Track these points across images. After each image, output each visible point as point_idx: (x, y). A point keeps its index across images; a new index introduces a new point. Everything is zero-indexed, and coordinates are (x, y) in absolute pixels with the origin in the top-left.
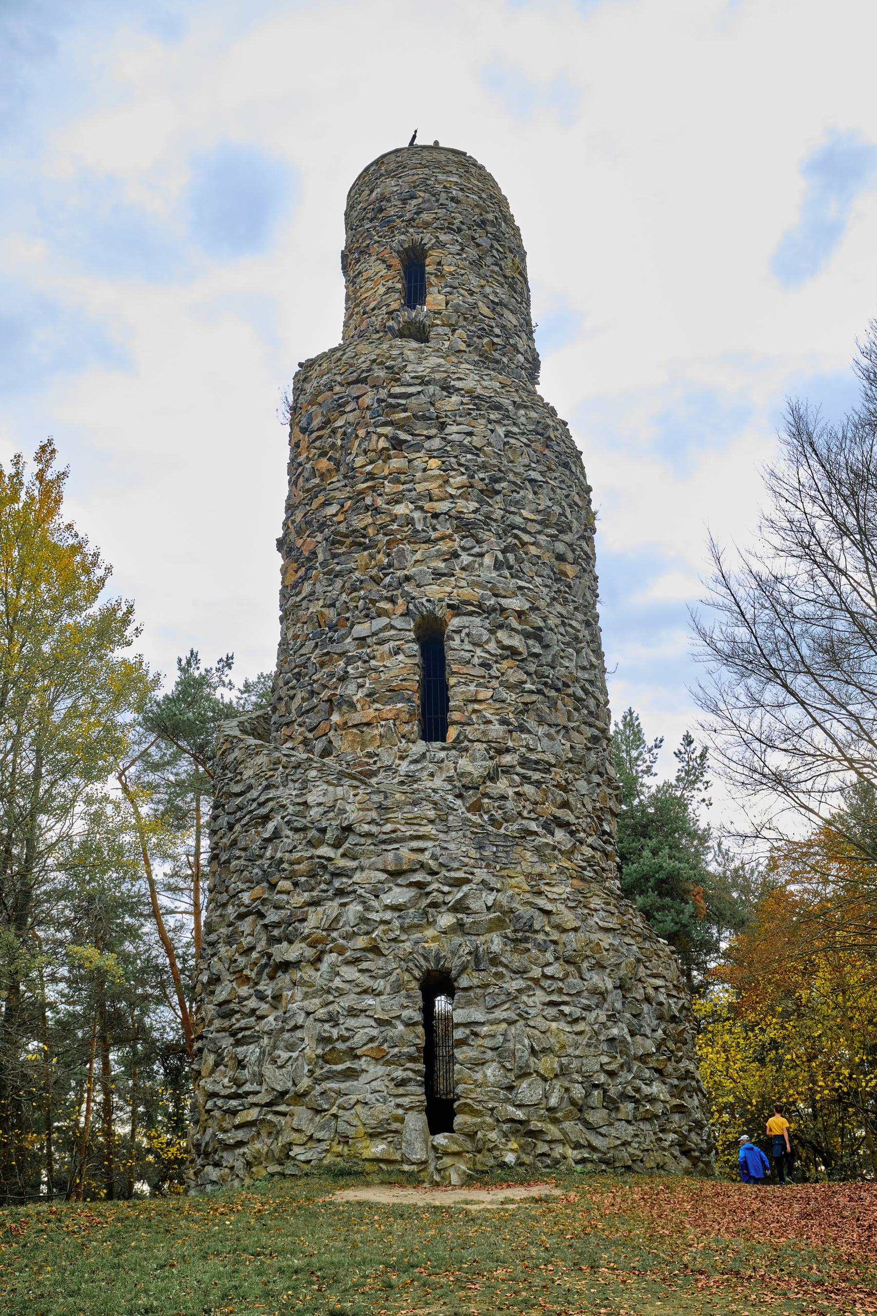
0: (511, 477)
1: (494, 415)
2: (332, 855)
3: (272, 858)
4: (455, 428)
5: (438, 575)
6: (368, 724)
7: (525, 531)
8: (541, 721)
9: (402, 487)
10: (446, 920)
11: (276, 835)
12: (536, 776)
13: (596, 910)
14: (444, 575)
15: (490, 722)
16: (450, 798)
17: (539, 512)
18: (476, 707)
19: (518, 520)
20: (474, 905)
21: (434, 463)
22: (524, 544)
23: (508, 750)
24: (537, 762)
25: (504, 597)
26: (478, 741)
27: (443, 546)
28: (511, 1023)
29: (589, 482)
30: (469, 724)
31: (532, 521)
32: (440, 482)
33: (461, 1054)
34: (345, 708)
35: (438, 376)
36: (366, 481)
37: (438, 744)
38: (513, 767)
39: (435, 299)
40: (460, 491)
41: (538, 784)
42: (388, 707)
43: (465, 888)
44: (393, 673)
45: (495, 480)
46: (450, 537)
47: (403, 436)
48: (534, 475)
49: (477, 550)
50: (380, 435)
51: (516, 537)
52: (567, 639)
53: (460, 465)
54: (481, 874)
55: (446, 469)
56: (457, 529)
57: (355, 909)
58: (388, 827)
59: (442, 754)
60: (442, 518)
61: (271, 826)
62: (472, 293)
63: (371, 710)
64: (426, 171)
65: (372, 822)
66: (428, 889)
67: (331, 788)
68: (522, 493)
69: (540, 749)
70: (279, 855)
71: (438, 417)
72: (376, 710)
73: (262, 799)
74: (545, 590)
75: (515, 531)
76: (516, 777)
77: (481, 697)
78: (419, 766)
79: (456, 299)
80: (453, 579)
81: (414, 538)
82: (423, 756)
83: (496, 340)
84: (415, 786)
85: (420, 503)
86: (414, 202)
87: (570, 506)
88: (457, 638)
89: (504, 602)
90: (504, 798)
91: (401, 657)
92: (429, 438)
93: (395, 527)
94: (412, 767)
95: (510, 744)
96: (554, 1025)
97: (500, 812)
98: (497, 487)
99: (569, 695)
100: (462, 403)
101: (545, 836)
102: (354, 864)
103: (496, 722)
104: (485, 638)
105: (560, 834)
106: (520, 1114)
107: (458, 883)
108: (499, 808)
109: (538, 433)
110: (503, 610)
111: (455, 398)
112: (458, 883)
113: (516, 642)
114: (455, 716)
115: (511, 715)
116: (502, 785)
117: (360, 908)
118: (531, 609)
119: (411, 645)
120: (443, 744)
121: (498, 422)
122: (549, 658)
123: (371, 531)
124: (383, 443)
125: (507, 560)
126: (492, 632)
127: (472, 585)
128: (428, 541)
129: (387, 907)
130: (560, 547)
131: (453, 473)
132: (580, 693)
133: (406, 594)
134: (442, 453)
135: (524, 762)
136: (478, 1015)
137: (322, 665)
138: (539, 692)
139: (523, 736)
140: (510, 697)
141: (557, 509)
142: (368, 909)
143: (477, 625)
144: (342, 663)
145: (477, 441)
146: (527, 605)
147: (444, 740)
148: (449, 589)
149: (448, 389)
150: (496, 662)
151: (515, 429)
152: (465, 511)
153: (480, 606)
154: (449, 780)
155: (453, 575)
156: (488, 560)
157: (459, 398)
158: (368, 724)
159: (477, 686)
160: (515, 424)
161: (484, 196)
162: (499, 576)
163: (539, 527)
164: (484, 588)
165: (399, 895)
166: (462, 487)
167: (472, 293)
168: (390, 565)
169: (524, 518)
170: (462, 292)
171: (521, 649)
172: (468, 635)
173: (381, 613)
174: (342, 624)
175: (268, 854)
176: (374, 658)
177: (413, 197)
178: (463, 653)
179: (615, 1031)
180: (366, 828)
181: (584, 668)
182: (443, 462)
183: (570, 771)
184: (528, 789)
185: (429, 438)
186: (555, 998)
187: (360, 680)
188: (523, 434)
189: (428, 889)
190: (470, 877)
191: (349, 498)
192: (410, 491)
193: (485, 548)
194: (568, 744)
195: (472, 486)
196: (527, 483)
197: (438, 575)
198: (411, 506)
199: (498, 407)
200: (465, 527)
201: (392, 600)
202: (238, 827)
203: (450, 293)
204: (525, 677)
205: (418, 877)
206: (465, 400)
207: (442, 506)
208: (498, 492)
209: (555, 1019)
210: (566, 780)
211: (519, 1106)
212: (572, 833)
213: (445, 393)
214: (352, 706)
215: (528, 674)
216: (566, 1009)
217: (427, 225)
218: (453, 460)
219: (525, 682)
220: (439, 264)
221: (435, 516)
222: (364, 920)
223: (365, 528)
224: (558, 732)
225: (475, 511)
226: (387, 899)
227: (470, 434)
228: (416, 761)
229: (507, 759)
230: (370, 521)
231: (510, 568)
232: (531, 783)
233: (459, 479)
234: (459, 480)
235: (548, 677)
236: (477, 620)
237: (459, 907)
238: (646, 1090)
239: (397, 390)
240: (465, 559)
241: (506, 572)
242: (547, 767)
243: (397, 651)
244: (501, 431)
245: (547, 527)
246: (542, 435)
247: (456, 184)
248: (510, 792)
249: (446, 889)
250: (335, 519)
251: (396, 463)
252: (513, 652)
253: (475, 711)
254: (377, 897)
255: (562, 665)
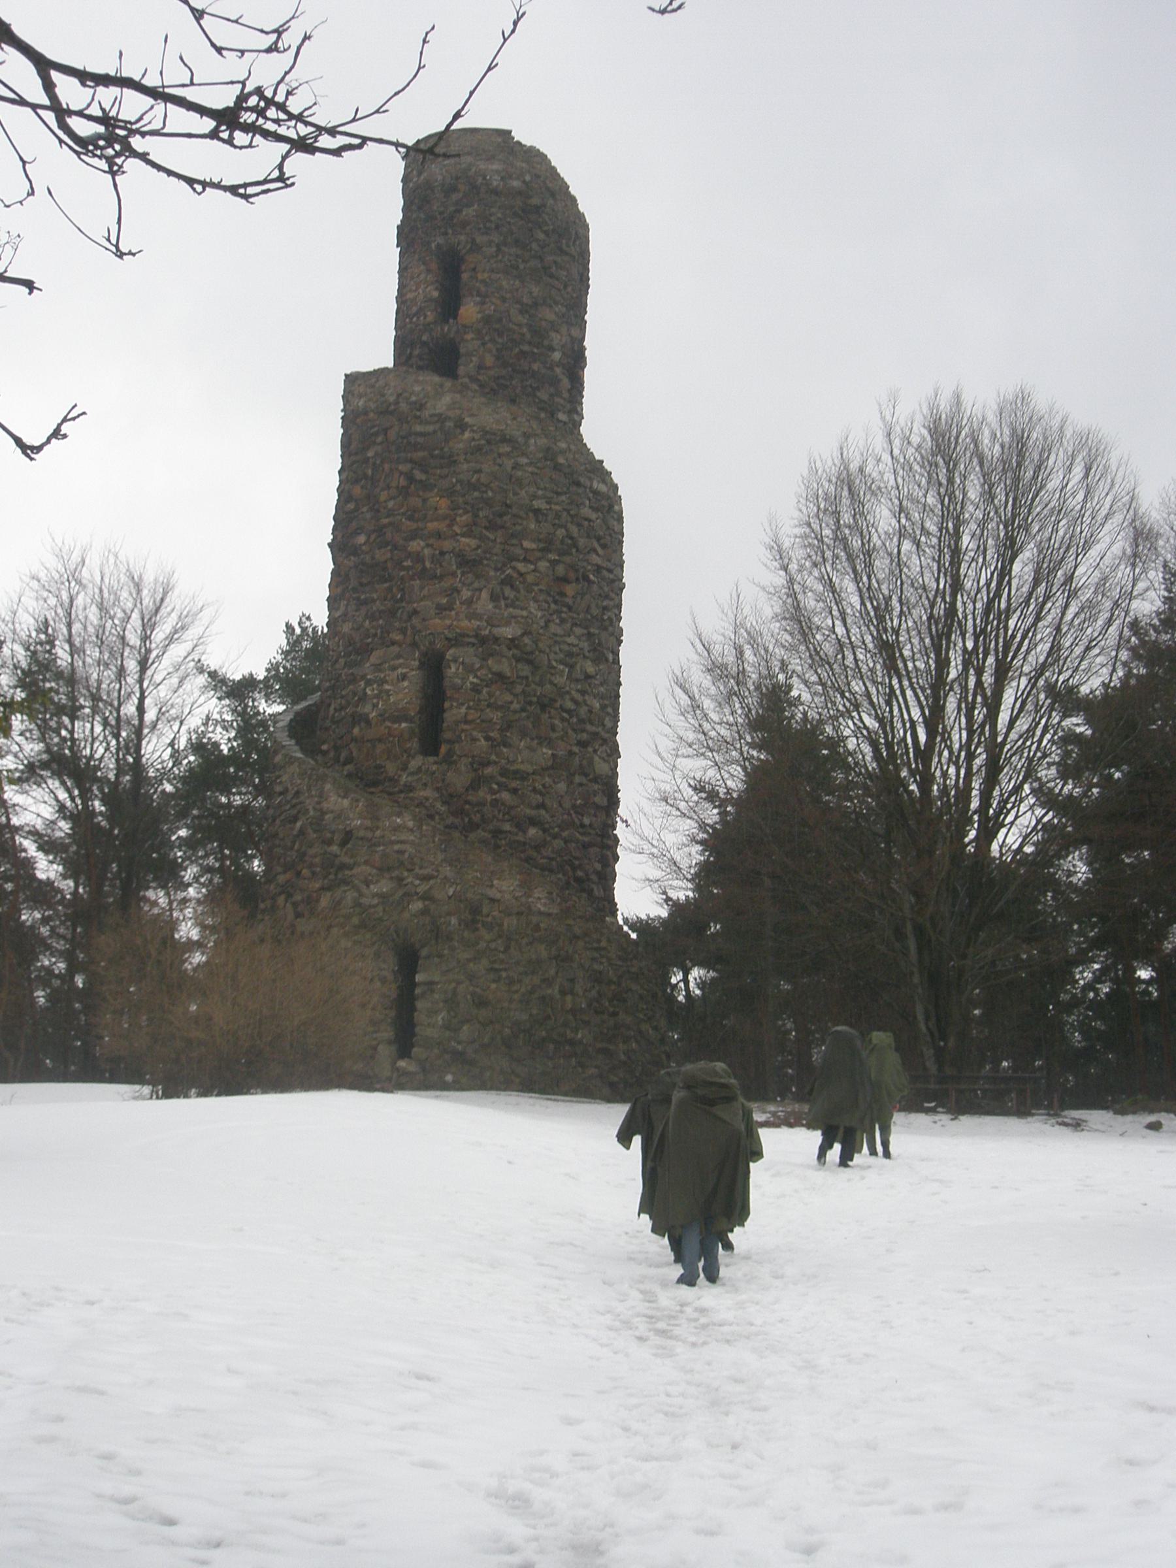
0: (514, 510)
1: (506, 448)
2: (338, 853)
3: (298, 851)
4: (465, 466)
5: (441, 609)
6: (380, 740)
7: (526, 560)
8: (524, 734)
9: (414, 526)
10: (416, 906)
11: (302, 832)
12: (514, 784)
13: (539, 898)
14: (445, 609)
15: (474, 740)
16: (438, 805)
17: (540, 540)
18: (465, 727)
19: (518, 551)
20: (438, 894)
21: (444, 503)
22: (521, 575)
23: (489, 763)
24: (516, 772)
25: (498, 626)
26: (465, 756)
27: (446, 584)
28: (459, 983)
29: (616, 481)
30: (458, 742)
31: (533, 550)
32: (447, 522)
33: (420, 1005)
34: (363, 724)
35: (451, 414)
36: (388, 516)
37: (431, 759)
38: (492, 777)
39: (469, 311)
40: (465, 529)
41: (515, 791)
42: (396, 726)
43: (432, 882)
44: (401, 696)
45: (501, 515)
46: (454, 574)
47: (419, 475)
48: (537, 504)
49: (476, 585)
50: (401, 473)
51: (514, 568)
52: (562, 656)
53: (466, 503)
54: (447, 871)
55: (454, 507)
56: (460, 565)
57: (351, 895)
58: (378, 833)
59: (434, 768)
60: (447, 556)
61: (299, 824)
62: (504, 300)
63: (383, 728)
64: (469, 159)
65: (366, 828)
66: (405, 882)
67: (340, 800)
68: (525, 523)
69: (520, 760)
70: (304, 849)
71: (450, 456)
72: (385, 728)
73: (294, 801)
74: (540, 614)
75: (514, 564)
76: (495, 786)
77: (470, 718)
78: (416, 777)
79: (490, 309)
80: (453, 613)
81: (423, 574)
82: (420, 768)
83: (526, 348)
84: (411, 795)
85: (431, 541)
86: (455, 197)
87: (579, 525)
88: (452, 665)
89: (496, 631)
90: (482, 804)
91: (406, 684)
92: (441, 477)
93: (408, 563)
94: (410, 779)
95: (493, 757)
96: (494, 986)
97: (478, 815)
98: (499, 521)
99: (556, 709)
100: (473, 439)
101: (517, 834)
102: (352, 861)
103: (482, 740)
104: (477, 666)
105: (532, 831)
106: (460, 1048)
107: (426, 878)
108: (478, 811)
109: (546, 460)
110: (496, 640)
111: (467, 435)
112: (426, 878)
113: (505, 667)
114: (447, 735)
115: (496, 732)
116: (482, 794)
117: (356, 894)
118: (523, 635)
119: (414, 673)
120: (435, 758)
121: (508, 455)
122: (537, 679)
123: (389, 564)
124: (403, 482)
125: (503, 594)
126: (484, 659)
127: (470, 617)
128: (435, 577)
129: (374, 895)
130: (560, 570)
131: (461, 511)
132: (569, 705)
133: (413, 627)
134: (450, 493)
135: (504, 773)
136: (436, 978)
137: (350, 682)
138: (523, 710)
139: (505, 750)
140: (496, 716)
141: (561, 533)
142: (361, 895)
143: (468, 655)
144: (362, 683)
145: (484, 479)
146: (519, 632)
147: (437, 755)
148: (448, 622)
149: (461, 426)
150: (487, 686)
151: (524, 460)
152: (467, 548)
153: (476, 636)
154: (438, 789)
155: (453, 609)
156: (485, 595)
157: (471, 435)
158: (380, 740)
159: (469, 708)
160: (524, 454)
161: (528, 178)
162: (495, 607)
163: (539, 554)
164: (481, 619)
165: (384, 886)
166: (467, 526)
167: (504, 300)
168: (402, 600)
169: (524, 549)
170: (494, 300)
171: (509, 674)
172: (463, 663)
173: (393, 643)
174: (366, 651)
175: (296, 847)
176: (386, 682)
177: (454, 189)
178: (456, 680)
179: (549, 991)
180: (362, 833)
181: (577, 680)
182: (452, 502)
183: (550, 776)
184: (505, 796)
185: (441, 477)
186: (496, 966)
187: (375, 701)
188: (531, 464)
189: (405, 882)
190: (436, 874)
191: (374, 531)
192: (422, 530)
193: (483, 582)
194: (550, 752)
195: (475, 524)
196: (531, 515)
197: (441, 609)
198: (422, 543)
199: (505, 440)
200: (466, 562)
201: (403, 631)
202: (278, 822)
203: (483, 303)
204: (509, 698)
205: (395, 873)
206: (477, 436)
207: (447, 545)
208: (502, 527)
209: (494, 981)
210: (544, 785)
211: (459, 1043)
212: (544, 831)
213: (459, 431)
214: (368, 722)
215: (516, 695)
216: (504, 974)
217: (464, 224)
218: (461, 500)
219: (511, 702)
220: (474, 269)
221: (442, 553)
222: (357, 904)
223: (386, 562)
224: (540, 744)
225: (479, 547)
226: (374, 889)
227: (479, 471)
228: (412, 774)
229: (489, 771)
230: (389, 555)
231: (506, 599)
232: (508, 790)
233: (464, 518)
234: (464, 519)
235: (535, 695)
236: (471, 650)
237: (426, 897)
238: (570, 1035)
239: (418, 428)
240: (466, 594)
241: (503, 603)
242: (523, 776)
243: (404, 677)
244: (508, 463)
245: (550, 551)
246: (552, 460)
247: (497, 172)
248: (489, 798)
249: (417, 882)
250: (364, 548)
251: (415, 501)
252: (500, 676)
253: (463, 731)
254: (368, 886)
255: (551, 683)
